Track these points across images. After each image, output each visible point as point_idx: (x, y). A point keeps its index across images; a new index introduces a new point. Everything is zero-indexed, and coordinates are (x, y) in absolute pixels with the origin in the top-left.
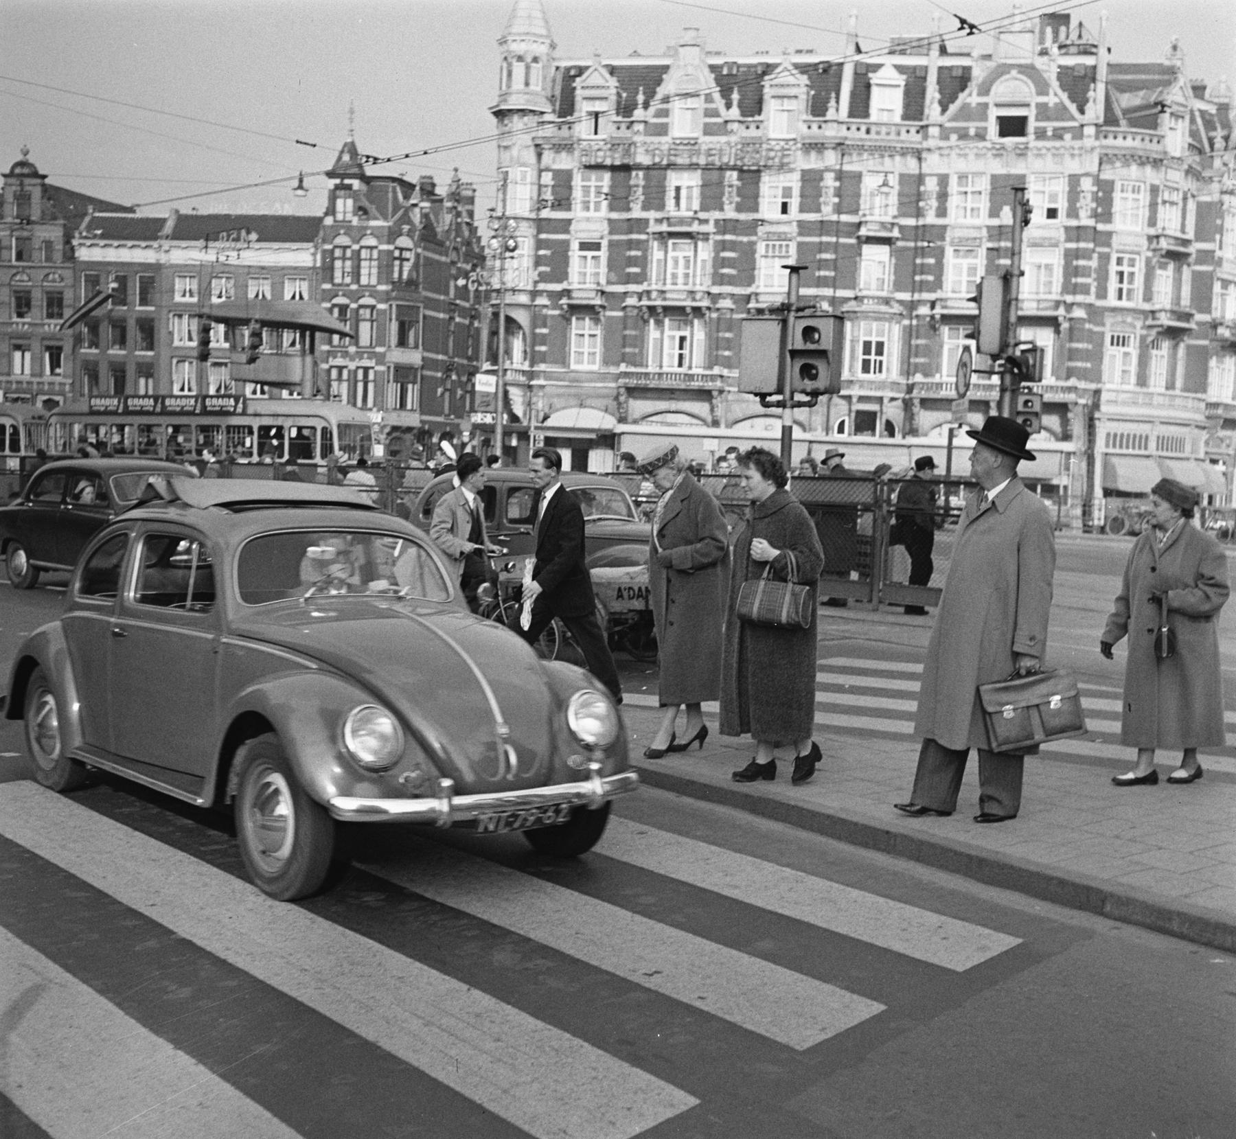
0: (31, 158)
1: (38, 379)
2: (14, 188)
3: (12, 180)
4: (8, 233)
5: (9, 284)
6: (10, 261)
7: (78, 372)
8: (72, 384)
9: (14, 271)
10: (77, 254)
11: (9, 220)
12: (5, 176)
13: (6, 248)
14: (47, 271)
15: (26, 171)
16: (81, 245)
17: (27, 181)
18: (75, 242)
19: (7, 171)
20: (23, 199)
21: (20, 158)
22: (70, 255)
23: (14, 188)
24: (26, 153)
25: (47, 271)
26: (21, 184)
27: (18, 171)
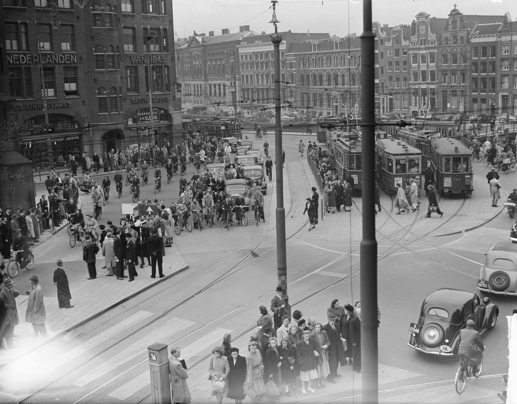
0: (457, 8)
1: (459, 85)
2: (452, 19)
3: (451, 17)
4: (450, 35)
5: (451, 53)
6: (451, 44)
7: (471, 82)
8: (469, 86)
9: (452, 48)
10: (471, 40)
11: (450, 30)
12: (448, 15)
13: (449, 40)
14: (462, 47)
15: (455, 13)
16: (472, 37)
17: (456, 16)
18: (470, 37)
19: (449, 14)
20: (454, 22)
21: (453, 8)
22: (468, 41)
23: (452, 19)
24: (455, 6)
25: (462, 47)
26: (454, 18)
27: (453, 13)
